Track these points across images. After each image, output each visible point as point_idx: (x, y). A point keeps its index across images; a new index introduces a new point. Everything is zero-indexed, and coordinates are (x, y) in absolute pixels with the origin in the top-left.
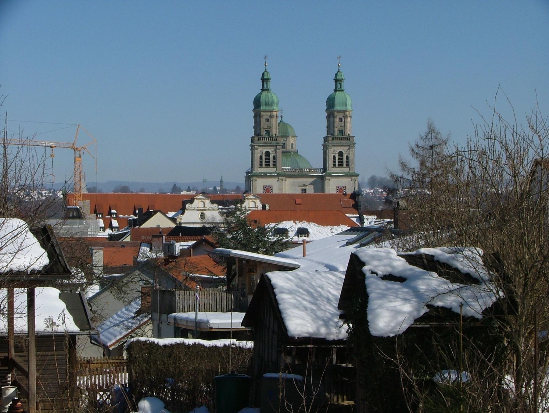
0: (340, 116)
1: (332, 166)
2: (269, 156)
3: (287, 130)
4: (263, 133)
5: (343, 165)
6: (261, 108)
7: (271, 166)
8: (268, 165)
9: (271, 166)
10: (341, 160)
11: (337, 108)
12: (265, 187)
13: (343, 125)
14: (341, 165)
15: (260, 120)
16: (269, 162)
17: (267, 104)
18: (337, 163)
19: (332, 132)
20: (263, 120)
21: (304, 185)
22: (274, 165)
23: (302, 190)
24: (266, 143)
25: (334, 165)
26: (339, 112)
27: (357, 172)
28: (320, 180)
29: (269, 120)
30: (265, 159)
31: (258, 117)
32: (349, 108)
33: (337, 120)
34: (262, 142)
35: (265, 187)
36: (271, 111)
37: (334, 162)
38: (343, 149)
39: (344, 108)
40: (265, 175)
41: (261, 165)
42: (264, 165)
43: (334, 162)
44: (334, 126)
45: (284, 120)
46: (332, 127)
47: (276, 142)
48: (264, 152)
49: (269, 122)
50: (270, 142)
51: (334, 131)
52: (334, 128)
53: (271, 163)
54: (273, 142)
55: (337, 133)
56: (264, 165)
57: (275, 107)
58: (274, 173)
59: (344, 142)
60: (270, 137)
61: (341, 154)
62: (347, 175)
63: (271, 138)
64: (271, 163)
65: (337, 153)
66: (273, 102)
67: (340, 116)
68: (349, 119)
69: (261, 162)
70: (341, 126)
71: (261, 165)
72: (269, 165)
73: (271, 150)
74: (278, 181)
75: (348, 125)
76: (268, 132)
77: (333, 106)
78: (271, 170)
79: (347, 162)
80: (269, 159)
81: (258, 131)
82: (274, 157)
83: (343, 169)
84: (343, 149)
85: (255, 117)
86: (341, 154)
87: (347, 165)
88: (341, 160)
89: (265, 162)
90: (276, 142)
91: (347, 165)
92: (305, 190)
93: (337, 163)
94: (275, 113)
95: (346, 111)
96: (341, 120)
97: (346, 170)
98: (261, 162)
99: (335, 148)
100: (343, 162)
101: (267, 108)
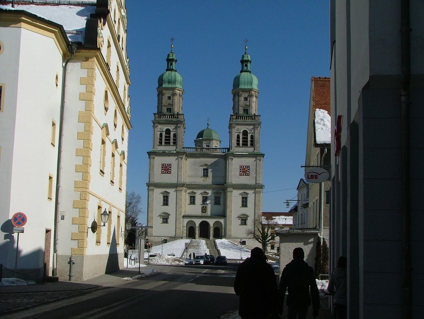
0: (246, 95)
2: (170, 134)
3: (212, 134)
4: (164, 110)
5: (247, 145)
6: (163, 86)
7: (172, 144)
8: (168, 143)
9: (172, 144)
11: (242, 87)
12: (163, 165)
14: (245, 144)
16: (169, 140)
17: (169, 82)
18: (241, 142)
19: (236, 111)
20: (165, 98)
21: (206, 165)
22: (174, 143)
23: (204, 169)
24: (166, 120)
25: (238, 144)
26: (244, 90)
27: (262, 152)
28: (222, 161)
29: (172, 98)
30: (166, 137)
33: (242, 99)
34: (163, 119)
35: (163, 165)
36: (174, 89)
37: (238, 141)
38: (248, 128)
39: (249, 87)
40: (164, 154)
41: (161, 143)
43: (238, 141)
44: (239, 105)
45: (209, 127)
46: (236, 107)
47: (177, 119)
48: (164, 130)
49: (171, 100)
50: (170, 119)
51: (239, 109)
52: (238, 107)
53: (172, 141)
54: (174, 120)
55: (241, 112)
56: (163, 143)
58: (173, 151)
59: (249, 121)
60: (172, 115)
61: (245, 133)
62: (250, 155)
63: (173, 115)
64: (172, 141)
65: (242, 131)
66: (175, 80)
67: (246, 95)
69: (161, 139)
70: (246, 105)
72: (169, 143)
73: (171, 128)
74: (178, 159)
76: (169, 110)
77: (238, 85)
78: (171, 148)
79: (252, 141)
80: (170, 137)
81: (160, 110)
83: (247, 148)
84: (248, 128)
85: (158, 95)
86: (245, 133)
90: (177, 119)
91: (252, 145)
93: (241, 142)
94: (178, 91)
96: (246, 99)
97: (250, 150)
98: (161, 139)
99: (239, 127)
101: (170, 86)
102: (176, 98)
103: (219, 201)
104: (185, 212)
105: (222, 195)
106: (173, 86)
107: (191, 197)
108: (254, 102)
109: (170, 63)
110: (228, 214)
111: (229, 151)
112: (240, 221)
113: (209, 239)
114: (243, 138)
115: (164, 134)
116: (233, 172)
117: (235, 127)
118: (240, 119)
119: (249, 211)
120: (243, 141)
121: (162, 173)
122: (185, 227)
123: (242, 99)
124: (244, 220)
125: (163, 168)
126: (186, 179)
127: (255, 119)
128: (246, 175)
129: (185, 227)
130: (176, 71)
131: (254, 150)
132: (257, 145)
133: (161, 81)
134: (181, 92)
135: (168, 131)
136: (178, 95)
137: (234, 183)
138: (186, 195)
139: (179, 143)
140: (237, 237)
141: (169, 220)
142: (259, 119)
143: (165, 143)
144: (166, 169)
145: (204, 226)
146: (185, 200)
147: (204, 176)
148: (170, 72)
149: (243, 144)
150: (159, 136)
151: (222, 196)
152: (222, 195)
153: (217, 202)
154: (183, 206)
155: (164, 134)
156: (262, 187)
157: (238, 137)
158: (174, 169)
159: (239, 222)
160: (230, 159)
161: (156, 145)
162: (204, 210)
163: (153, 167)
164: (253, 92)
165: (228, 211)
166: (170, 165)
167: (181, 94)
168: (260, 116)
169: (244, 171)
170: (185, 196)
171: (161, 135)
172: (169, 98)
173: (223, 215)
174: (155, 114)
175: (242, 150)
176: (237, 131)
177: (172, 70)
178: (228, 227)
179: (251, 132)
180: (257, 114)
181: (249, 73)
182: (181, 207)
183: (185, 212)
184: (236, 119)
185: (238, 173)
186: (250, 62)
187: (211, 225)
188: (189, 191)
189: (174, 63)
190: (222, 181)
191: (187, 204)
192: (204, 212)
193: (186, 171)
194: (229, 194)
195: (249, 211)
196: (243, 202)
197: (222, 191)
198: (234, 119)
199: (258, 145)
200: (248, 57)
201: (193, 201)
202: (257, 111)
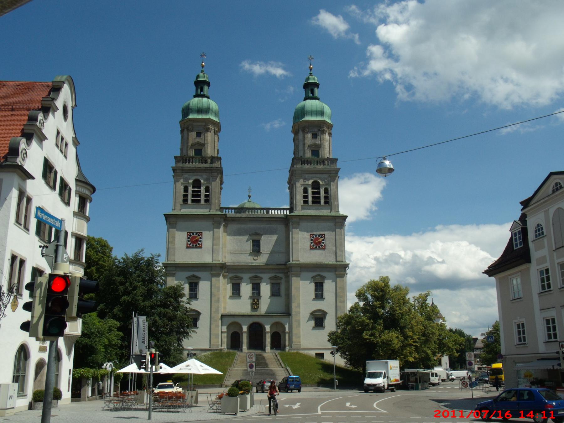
5: (319, 203)
7: (202, 202)
8: (196, 200)
9: (202, 202)
16: (199, 196)
18: (310, 199)
22: (207, 201)
25: (306, 202)
30: (193, 191)
31: (185, 131)
37: (306, 197)
41: (185, 201)
42: (190, 202)
43: (306, 197)
44: (304, 144)
47: (211, 165)
48: (191, 181)
49: (202, 137)
51: (304, 151)
52: (304, 147)
53: (202, 198)
56: (190, 202)
64: (202, 198)
69: (186, 196)
71: (185, 201)
72: (199, 201)
76: (198, 152)
79: (326, 198)
80: (200, 191)
81: (184, 151)
85: (182, 131)
86: (316, 185)
98: (186, 196)
100: (319, 198)
101: (200, 116)
103: (279, 289)
108: (327, 141)
109: (199, 87)
114: (313, 193)
116: (300, 244)
120: (313, 197)
121: (188, 247)
122: (224, 332)
124: (319, 319)
126: (225, 257)
128: (320, 249)
129: (224, 332)
130: (208, 98)
135: (197, 184)
136: (212, 131)
139: (214, 200)
141: (200, 323)
143: (193, 201)
145: (256, 332)
146: (225, 289)
147: (253, 250)
148: (200, 98)
149: (313, 202)
150: (182, 192)
151: (283, 282)
154: (221, 299)
162: (255, 304)
165: (294, 305)
169: (317, 243)
171: (186, 189)
173: (288, 313)
177: (203, 96)
181: (317, 101)
182: (218, 301)
183: (225, 308)
187: (268, 328)
188: (231, 275)
189: (206, 88)
191: (228, 297)
195: (327, 305)
199: (336, 203)
200: (314, 79)
201: (236, 292)
202: (331, 154)
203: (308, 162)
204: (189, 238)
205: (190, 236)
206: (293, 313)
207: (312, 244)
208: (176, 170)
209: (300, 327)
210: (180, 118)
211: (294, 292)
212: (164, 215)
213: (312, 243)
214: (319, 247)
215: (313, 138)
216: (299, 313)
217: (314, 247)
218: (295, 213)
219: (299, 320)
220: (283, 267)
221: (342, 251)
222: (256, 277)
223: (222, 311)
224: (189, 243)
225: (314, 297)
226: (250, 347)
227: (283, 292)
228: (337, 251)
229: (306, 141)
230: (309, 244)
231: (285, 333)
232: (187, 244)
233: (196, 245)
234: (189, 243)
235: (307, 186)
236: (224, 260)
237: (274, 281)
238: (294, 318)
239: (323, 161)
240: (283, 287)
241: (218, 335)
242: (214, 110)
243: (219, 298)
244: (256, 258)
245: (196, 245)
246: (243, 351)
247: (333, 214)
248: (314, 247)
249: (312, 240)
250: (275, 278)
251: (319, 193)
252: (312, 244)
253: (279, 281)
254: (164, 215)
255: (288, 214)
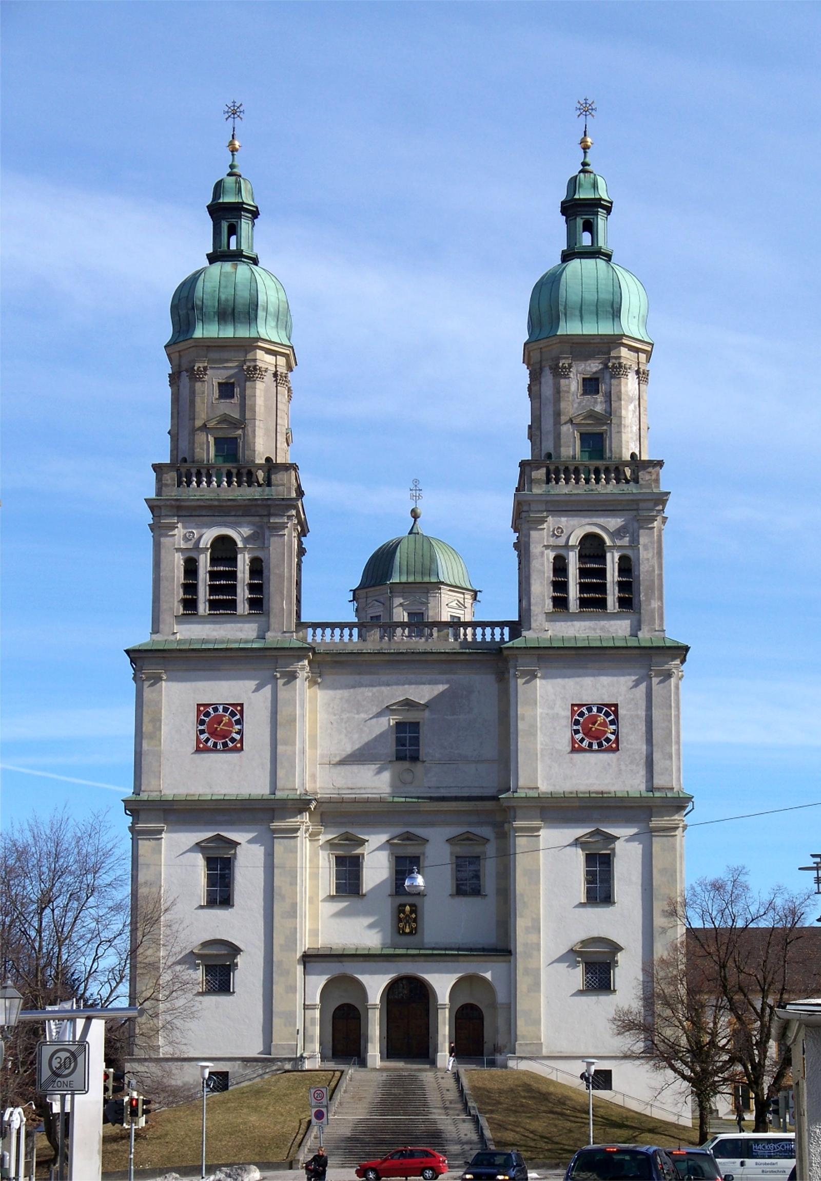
0: (594, 366)
1: (549, 605)
5: (601, 604)
6: (198, 333)
7: (243, 608)
8: (223, 604)
9: (243, 608)
10: (593, 578)
12: (203, 710)
13: (599, 408)
15: (193, 393)
16: (232, 589)
18: (573, 592)
19: (548, 446)
22: (257, 604)
25: (560, 603)
27: (674, 634)
30: (213, 575)
31: (185, 379)
32: (631, 325)
35: (203, 710)
37: (560, 586)
39: (605, 328)
41: (190, 604)
43: (560, 586)
44: (558, 414)
46: (548, 424)
47: (267, 492)
51: (558, 436)
52: (557, 423)
53: (243, 594)
56: (203, 608)
57: (266, 330)
59: (608, 488)
63: (246, 475)
64: (243, 594)
65: (574, 541)
68: (630, 384)
70: (592, 415)
72: (232, 605)
75: (628, 413)
80: (233, 575)
81: (184, 445)
82: (257, 568)
85: (174, 379)
86: (592, 548)
87: (627, 603)
88: (593, 578)
89: (213, 589)
90: (267, 492)
92: (415, 726)
93: (573, 592)
94: (270, 359)
95: (616, 341)
96: (591, 385)
98: (190, 588)
100: (602, 588)
101: (228, 332)
102: (262, 391)
103: (477, 876)
104: (315, 933)
105: (491, 849)
106: (243, 332)
107: (340, 861)
109: (225, 226)
110: (522, 938)
111: (515, 634)
112: (579, 971)
113: (433, 1063)
114: (583, 572)
115: (204, 563)
116: (540, 737)
117: (543, 521)
118: (567, 481)
119: (621, 922)
120: (583, 588)
122: (312, 1007)
123: (573, 384)
125: (202, 722)
126: (313, 777)
127: (636, 480)
129: (312, 1007)
130: (255, 261)
131: (636, 628)
132: (648, 604)
133: (186, 306)
134: (282, 361)
135: (224, 550)
136: (269, 377)
137: (544, 786)
138: (314, 855)
140: (568, 1050)
142: (657, 481)
143: (213, 605)
144: (219, 730)
148: (228, 267)
149: (584, 603)
152: (491, 849)
153: (467, 884)
155: (204, 563)
156: (680, 804)
157: (560, 567)
158: (255, 729)
159: (577, 976)
160: (524, 674)
161: (167, 619)
163: (157, 721)
164: (624, 352)
165: (521, 924)
166: (236, 710)
167: (282, 370)
168: (660, 464)
169: (594, 729)
170: (310, 860)
171: (191, 568)
172: (226, 390)
173: (502, 949)
174: (157, 468)
175: (579, 630)
176: (552, 541)
177: (237, 256)
178: (522, 1004)
179: (618, 543)
180: (645, 457)
181: (601, 263)
182: (292, 912)
184: (548, 481)
185: (564, 742)
186: (608, 210)
190: (486, 783)
191: (322, 895)
192: (404, 933)
193: (313, 738)
194: (522, 842)
195: (621, 922)
196: (591, 878)
197: (486, 831)
198: (538, 481)
199: (655, 604)
202: (645, 442)
203: (571, 471)
204: (202, 722)
205: (207, 714)
206: (520, 949)
207: (579, 737)
208: (159, 507)
209: (539, 991)
210: (166, 331)
211: (521, 884)
212: (127, 652)
213: (577, 732)
214: (600, 745)
215: (585, 392)
216: (538, 945)
217: (585, 744)
218: (530, 636)
219: (538, 970)
220: (489, 805)
221: (671, 757)
222: (408, 837)
223: (305, 943)
224: (203, 737)
225: (583, 900)
226: (391, 1052)
227: (489, 883)
228: (656, 756)
229: (563, 405)
230: (568, 734)
231: (493, 1005)
232: (198, 741)
233: (225, 745)
234: (203, 737)
235: (562, 552)
236: (308, 787)
237: (459, 850)
238: (521, 963)
239: (616, 471)
240: (489, 869)
241: (291, 1016)
242: (271, 309)
243: (294, 905)
244: (408, 777)
245: (225, 745)
246: (370, 1063)
247: (645, 636)
248: (585, 744)
249: (577, 722)
250: (467, 838)
251: (602, 573)
252: (579, 737)
253: (476, 850)
254: (127, 652)
255: (507, 638)
